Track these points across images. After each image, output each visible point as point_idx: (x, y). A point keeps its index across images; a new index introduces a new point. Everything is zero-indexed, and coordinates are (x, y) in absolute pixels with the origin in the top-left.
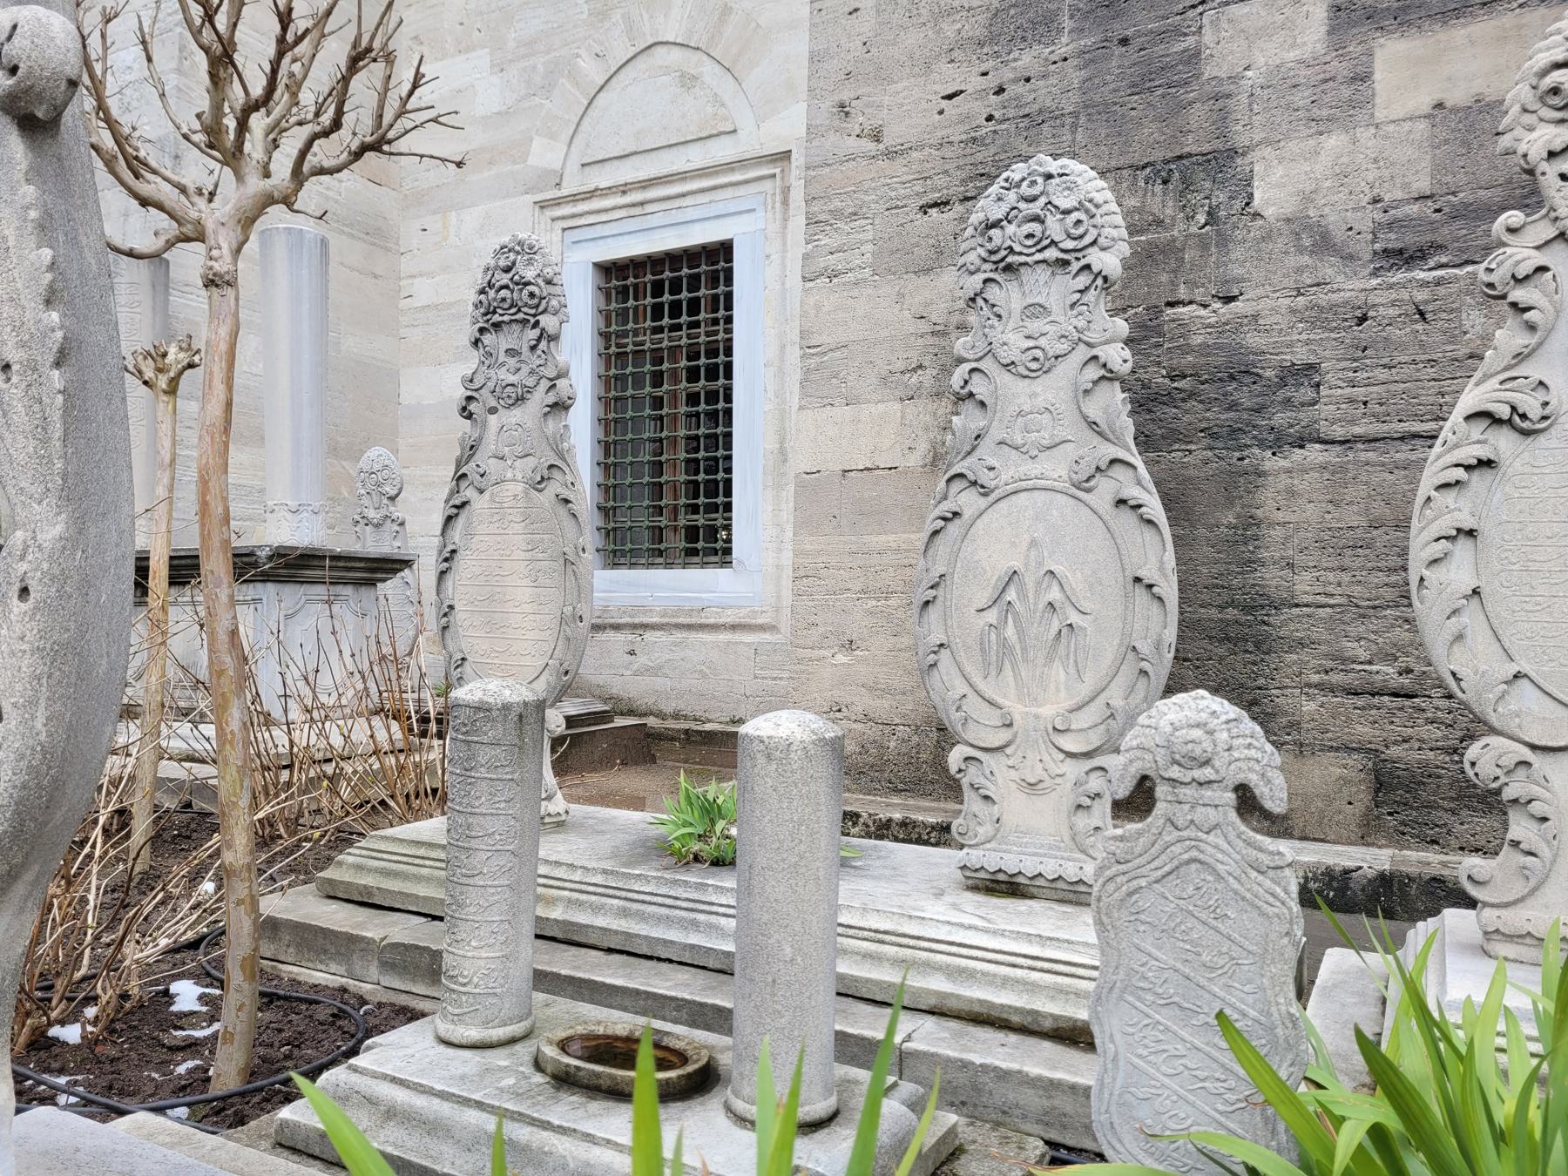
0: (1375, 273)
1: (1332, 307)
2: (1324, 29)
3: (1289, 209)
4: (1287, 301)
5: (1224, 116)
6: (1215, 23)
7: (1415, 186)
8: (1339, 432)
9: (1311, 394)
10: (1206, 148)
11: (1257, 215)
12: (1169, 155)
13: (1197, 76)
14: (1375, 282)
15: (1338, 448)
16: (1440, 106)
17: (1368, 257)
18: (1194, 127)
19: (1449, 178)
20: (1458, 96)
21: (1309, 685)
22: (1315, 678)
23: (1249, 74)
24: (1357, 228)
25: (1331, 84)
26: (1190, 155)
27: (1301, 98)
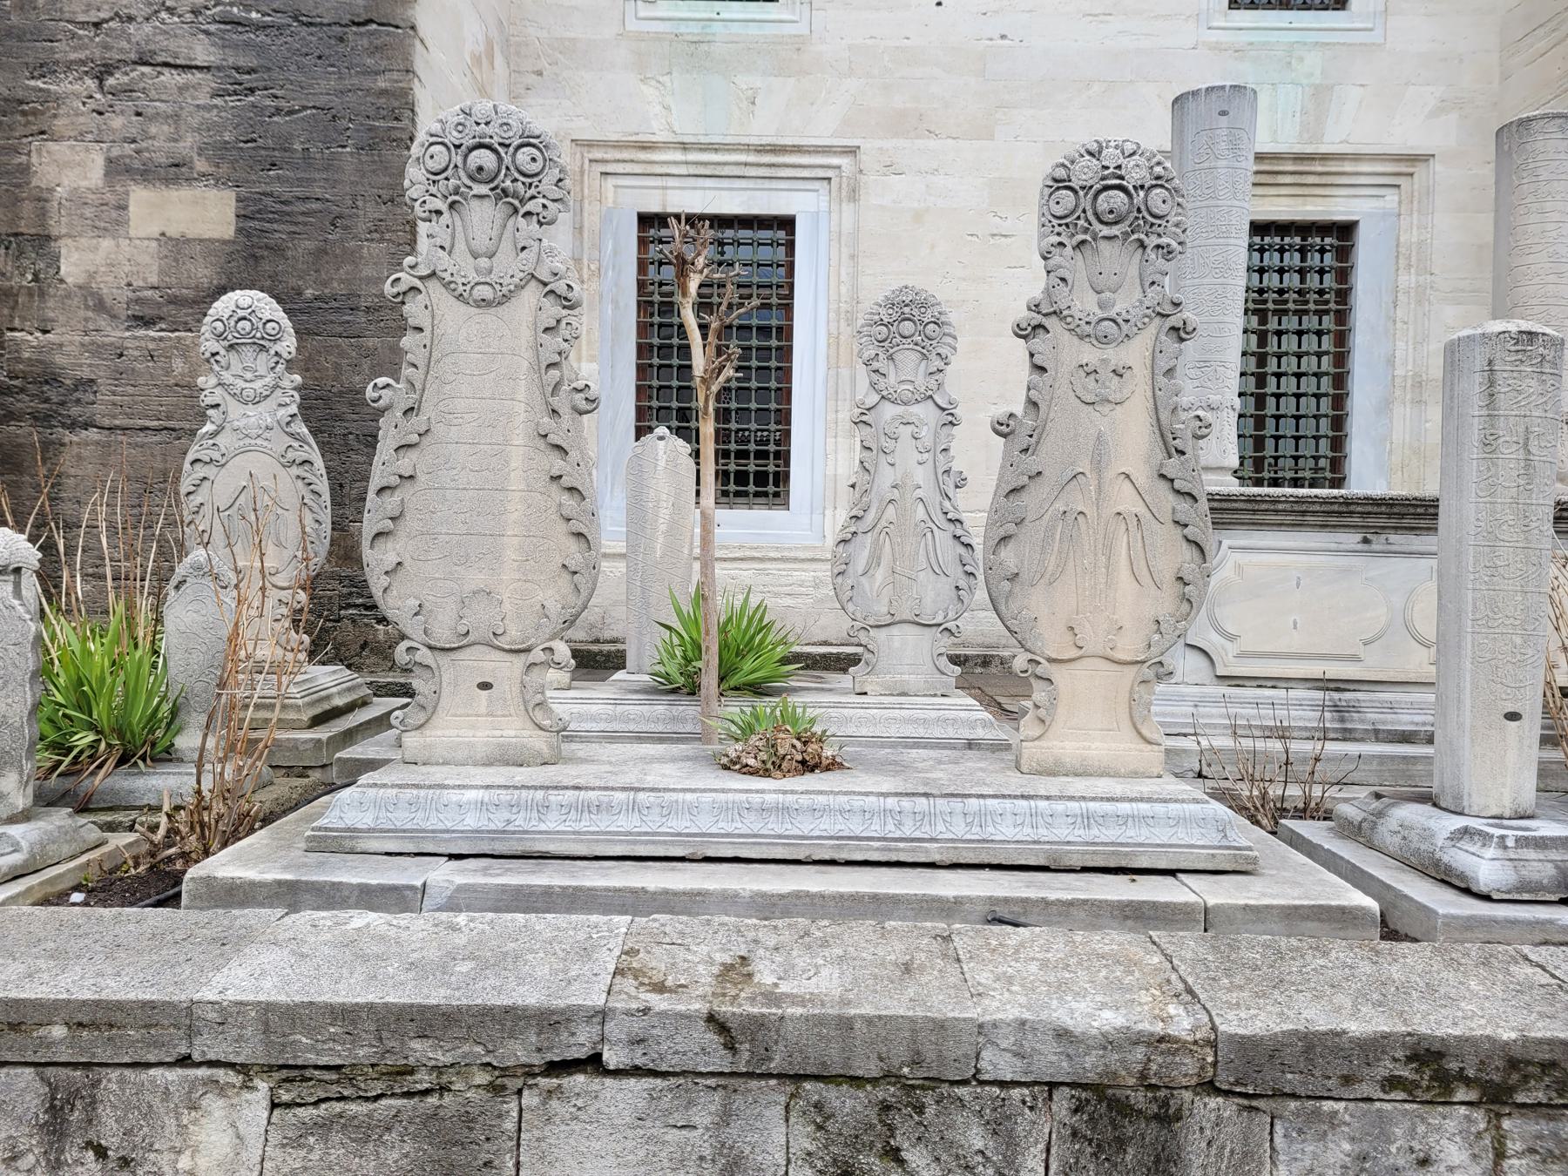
0: (128, 329)
1: (104, 345)
2: (102, 172)
3: (81, 281)
4: (79, 338)
5: (43, 214)
6: (39, 151)
7: (150, 280)
8: (106, 422)
9: (92, 397)
10: (33, 231)
11: (62, 281)
12: (10, 231)
13: (28, 183)
14: (127, 334)
15: (107, 432)
16: (163, 234)
17: (124, 318)
18: (26, 216)
19: (167, 279)
20: (173, 232)
21: (87, 575)
22: (90, 571)
23: (58, 189)
24: (119, 299)
25: (105, 208)
26: (22, 234)
27: (88, 212)
